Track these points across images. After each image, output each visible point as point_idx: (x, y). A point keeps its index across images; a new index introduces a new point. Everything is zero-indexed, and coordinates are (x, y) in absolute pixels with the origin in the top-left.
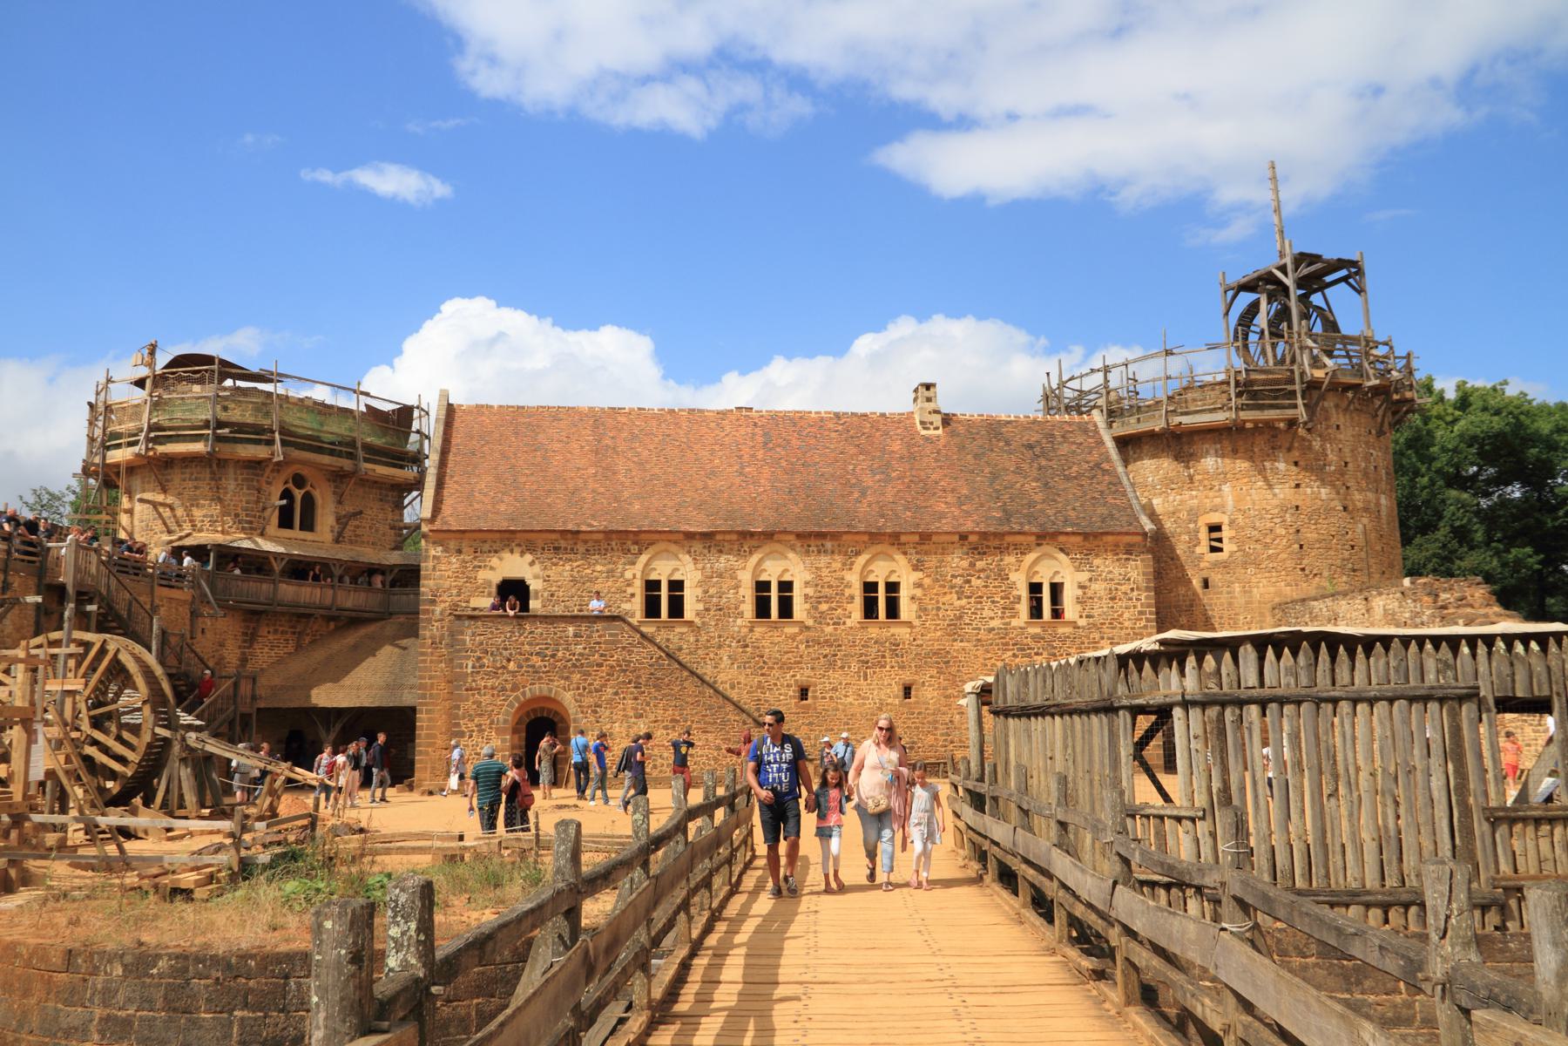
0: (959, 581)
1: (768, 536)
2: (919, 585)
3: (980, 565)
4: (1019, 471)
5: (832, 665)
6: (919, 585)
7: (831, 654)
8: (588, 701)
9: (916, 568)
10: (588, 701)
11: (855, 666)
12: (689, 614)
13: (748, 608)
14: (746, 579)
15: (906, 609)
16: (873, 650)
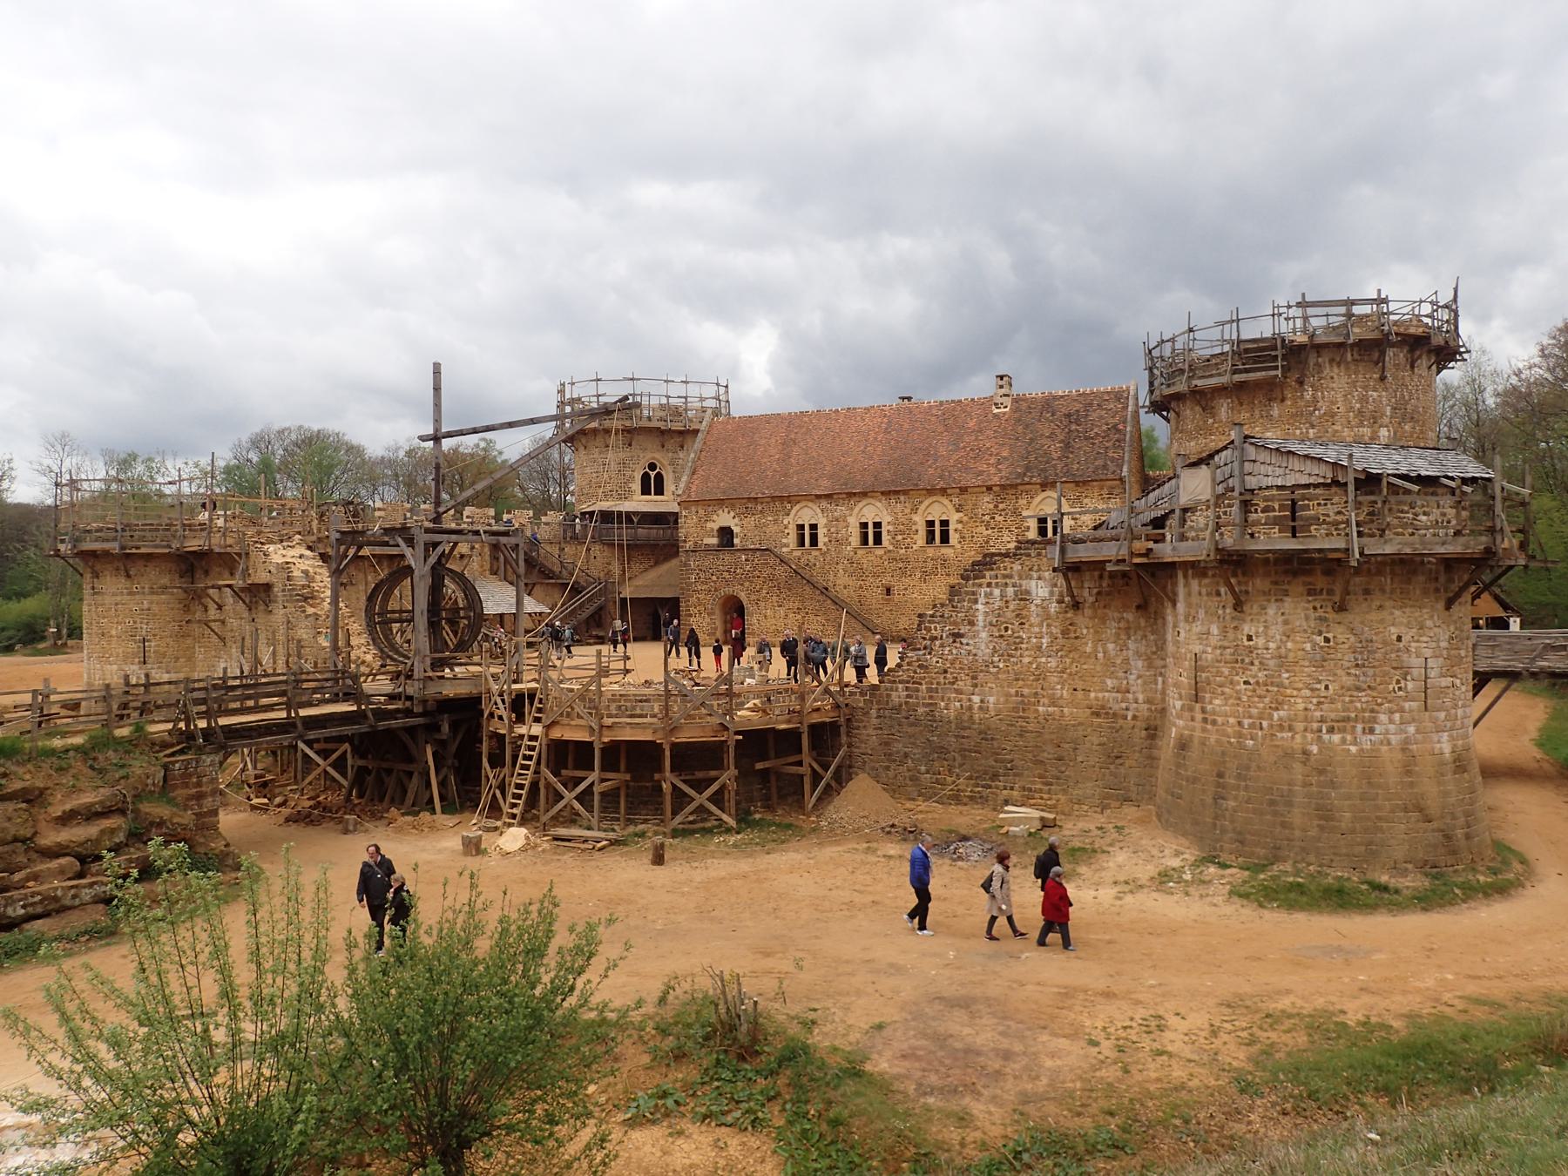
0: (987, 518)
1: (864, 494)
2: (960, 522)
3: (1001, 506)
4: (1052, 436)
5: (904, 573)
6: (960, 522)
7: (904, 566)
8: (753, 597)
9: (958, 511)
10: (753, 597)
11: (918, 575)
12: (820, 545)
13: (855, 540)
14: (854, 522)
15: (954, 538)
16: (930, 564)
